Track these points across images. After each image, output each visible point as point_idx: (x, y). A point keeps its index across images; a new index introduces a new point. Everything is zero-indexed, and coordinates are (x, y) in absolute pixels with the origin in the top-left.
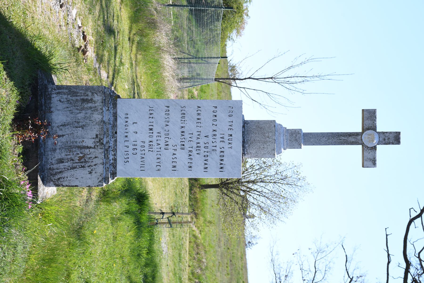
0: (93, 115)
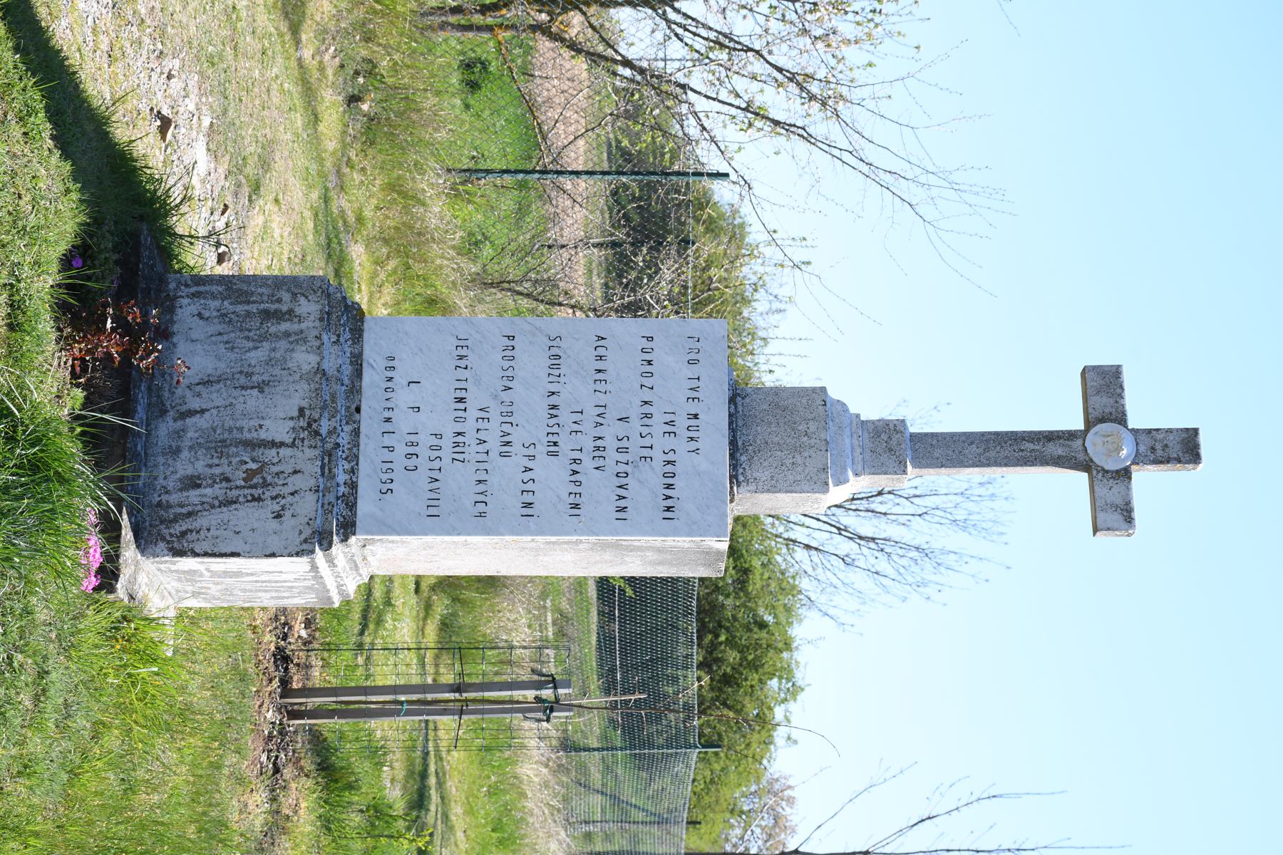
0: (294, 355)
